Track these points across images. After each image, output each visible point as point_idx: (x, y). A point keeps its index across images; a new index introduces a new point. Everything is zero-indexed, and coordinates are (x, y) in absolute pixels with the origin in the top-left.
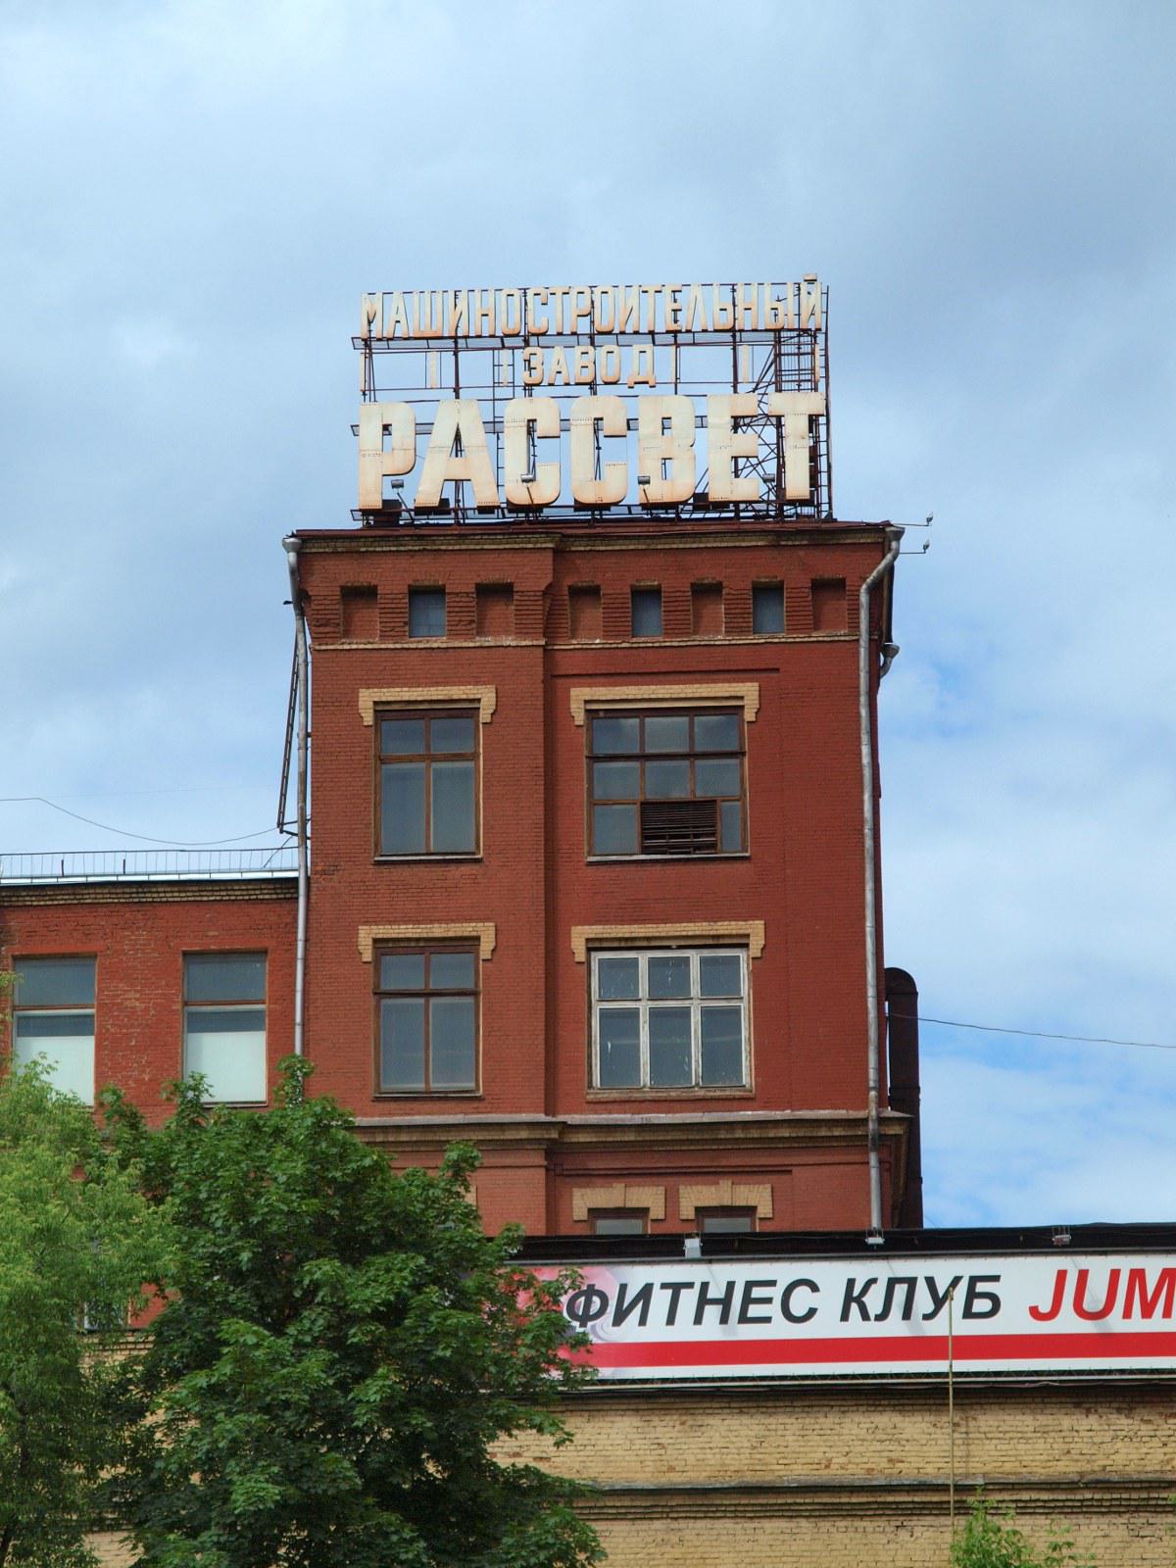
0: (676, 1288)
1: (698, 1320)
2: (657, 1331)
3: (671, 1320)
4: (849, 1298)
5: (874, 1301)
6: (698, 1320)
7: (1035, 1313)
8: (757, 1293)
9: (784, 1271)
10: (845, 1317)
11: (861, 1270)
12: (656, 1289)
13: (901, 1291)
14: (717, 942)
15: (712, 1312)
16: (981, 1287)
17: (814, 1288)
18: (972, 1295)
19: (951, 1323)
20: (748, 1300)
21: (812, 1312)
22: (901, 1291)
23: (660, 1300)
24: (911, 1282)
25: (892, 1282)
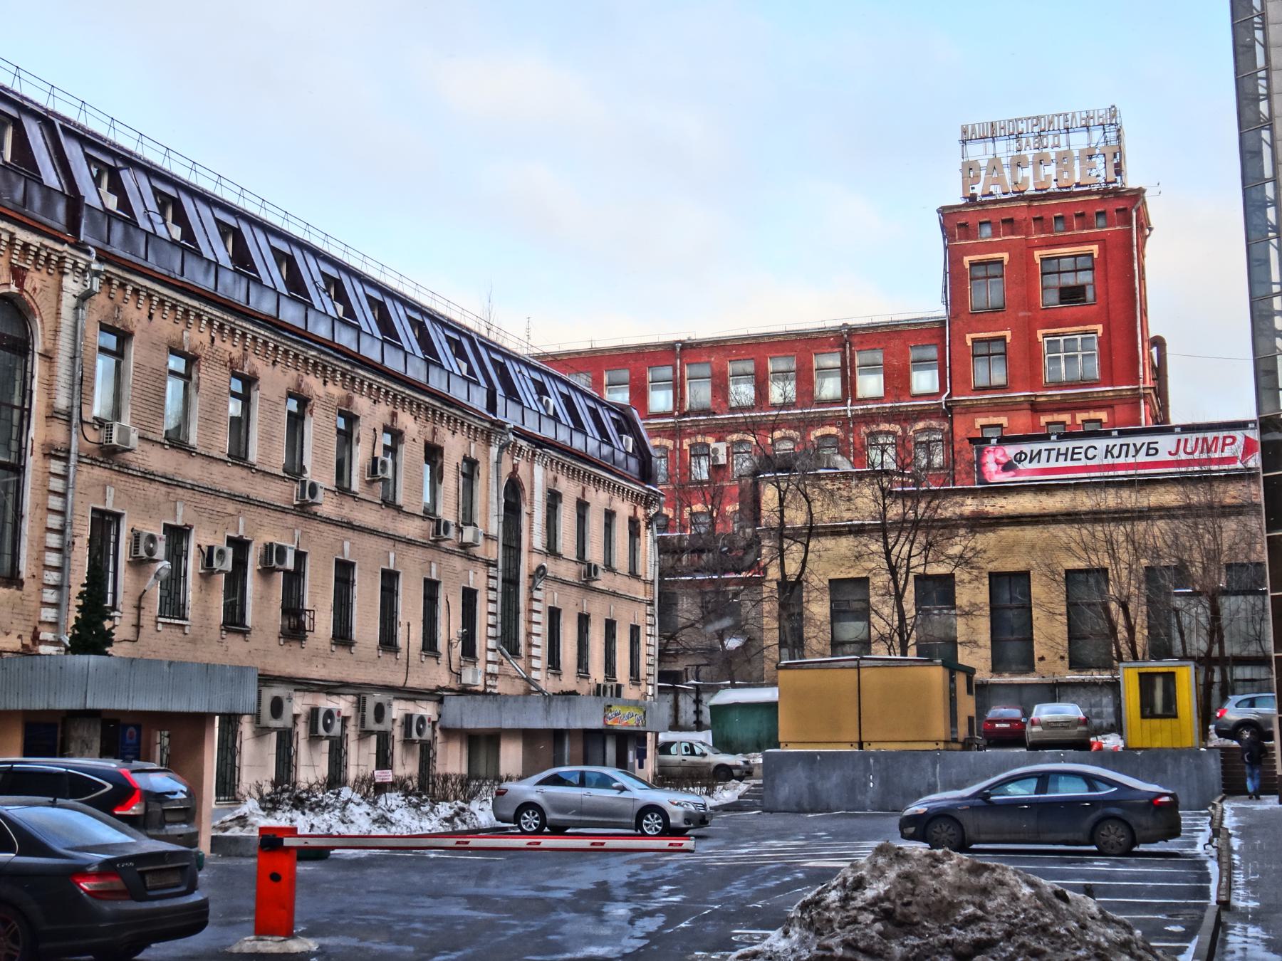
0: (1049, 450)
1: (1057, 460)
2: (1043, 464)
3: (1048, 461)
4: (1107, 451)
5: (1116, 452)
6: (1057, 460)
7: (1170, 453)
8: (1076, 451)
9: (1085, 443)
10: (1106, 457)
11: (1111, 442)
12: (1043, 452)
13: (1125, 448)
14: (1086, 332)
15: (1062, 457)
16: (1152, 446)
17: (1095, 448)
18: (1149, 448)
19: (1142, 458)
20: (1073, 453)
21: (1095, 456)
22: (1125, 448)
23: (1044, 455)
24: (1128, 445)
25: (1121, 446)
